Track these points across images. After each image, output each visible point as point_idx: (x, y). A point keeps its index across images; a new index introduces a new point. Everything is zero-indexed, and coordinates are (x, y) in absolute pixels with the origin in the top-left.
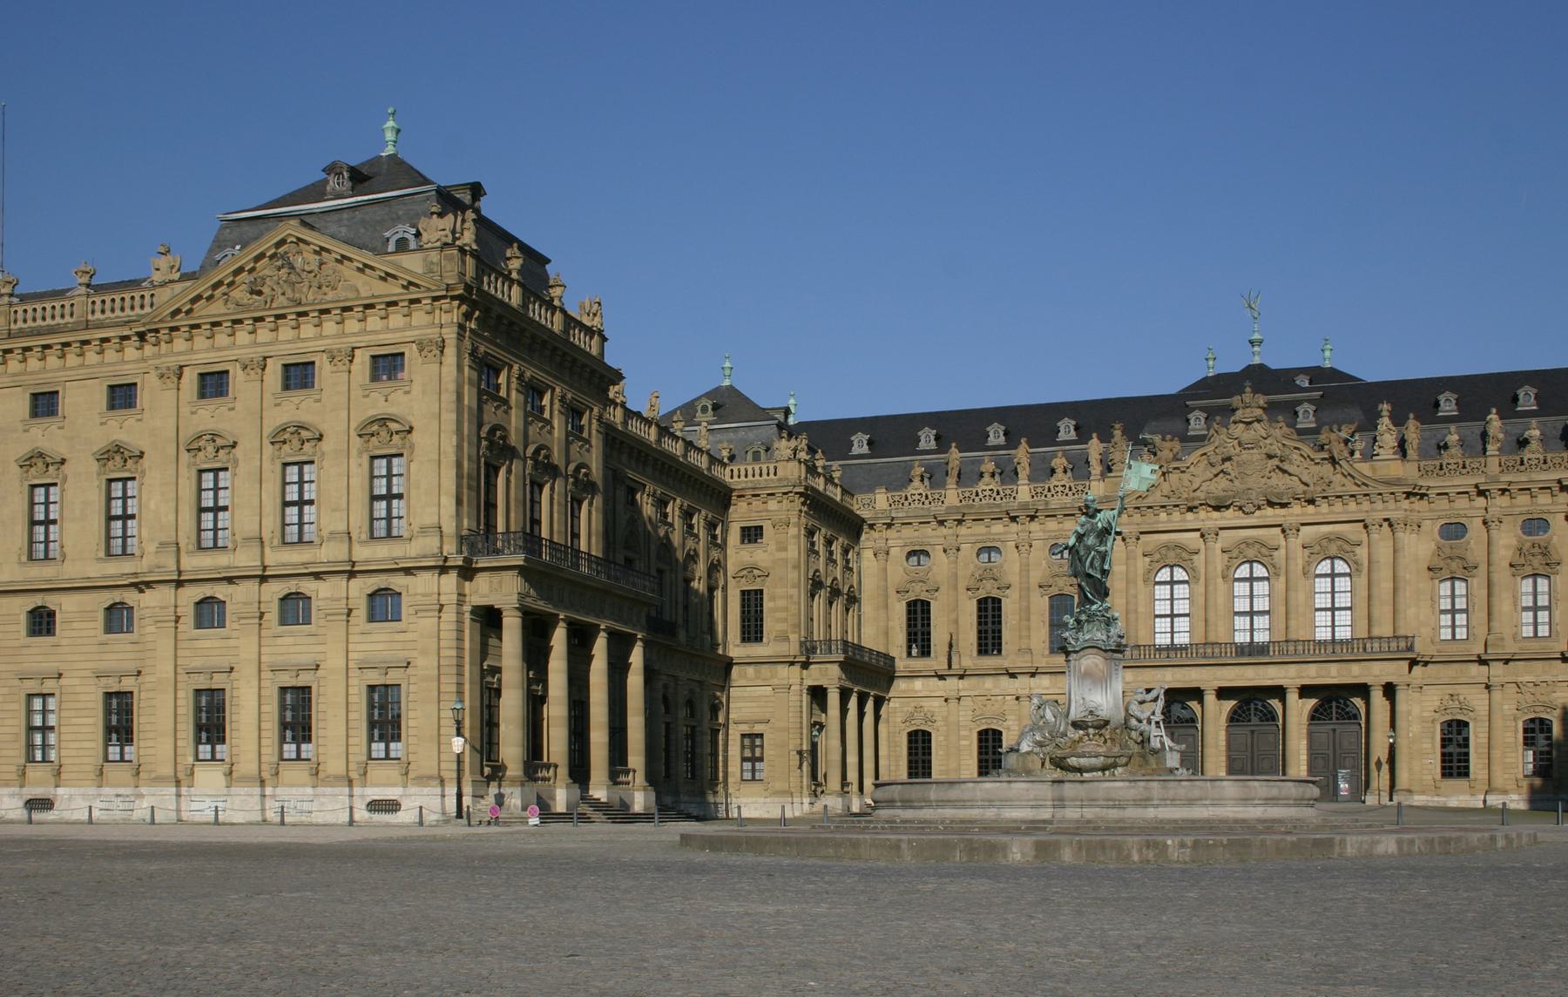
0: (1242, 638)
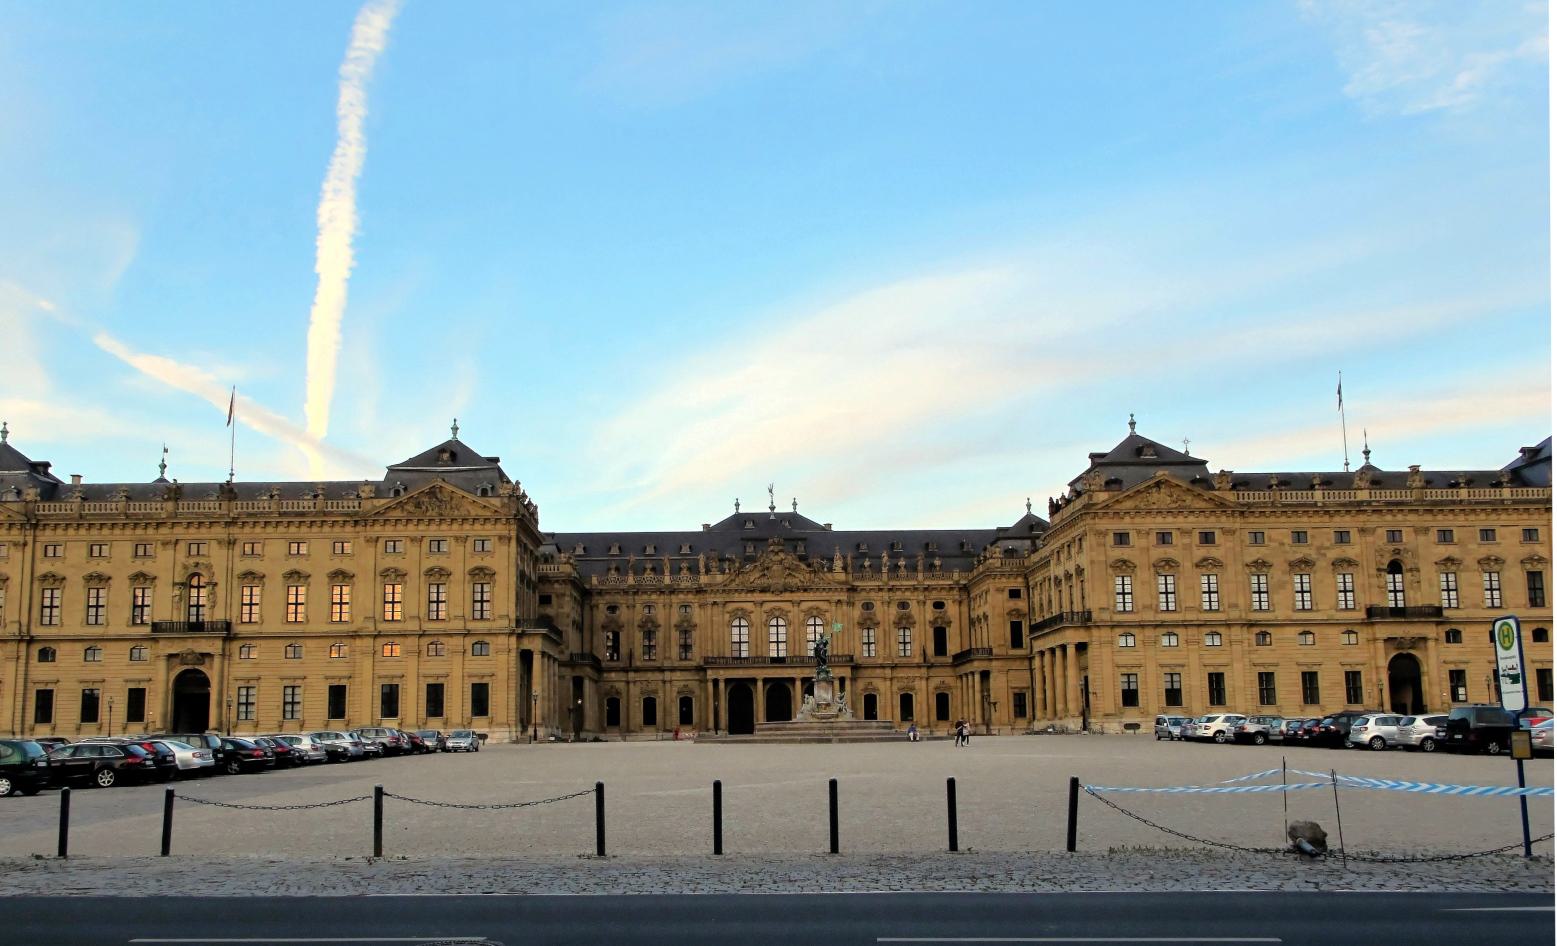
0: (773, 654)
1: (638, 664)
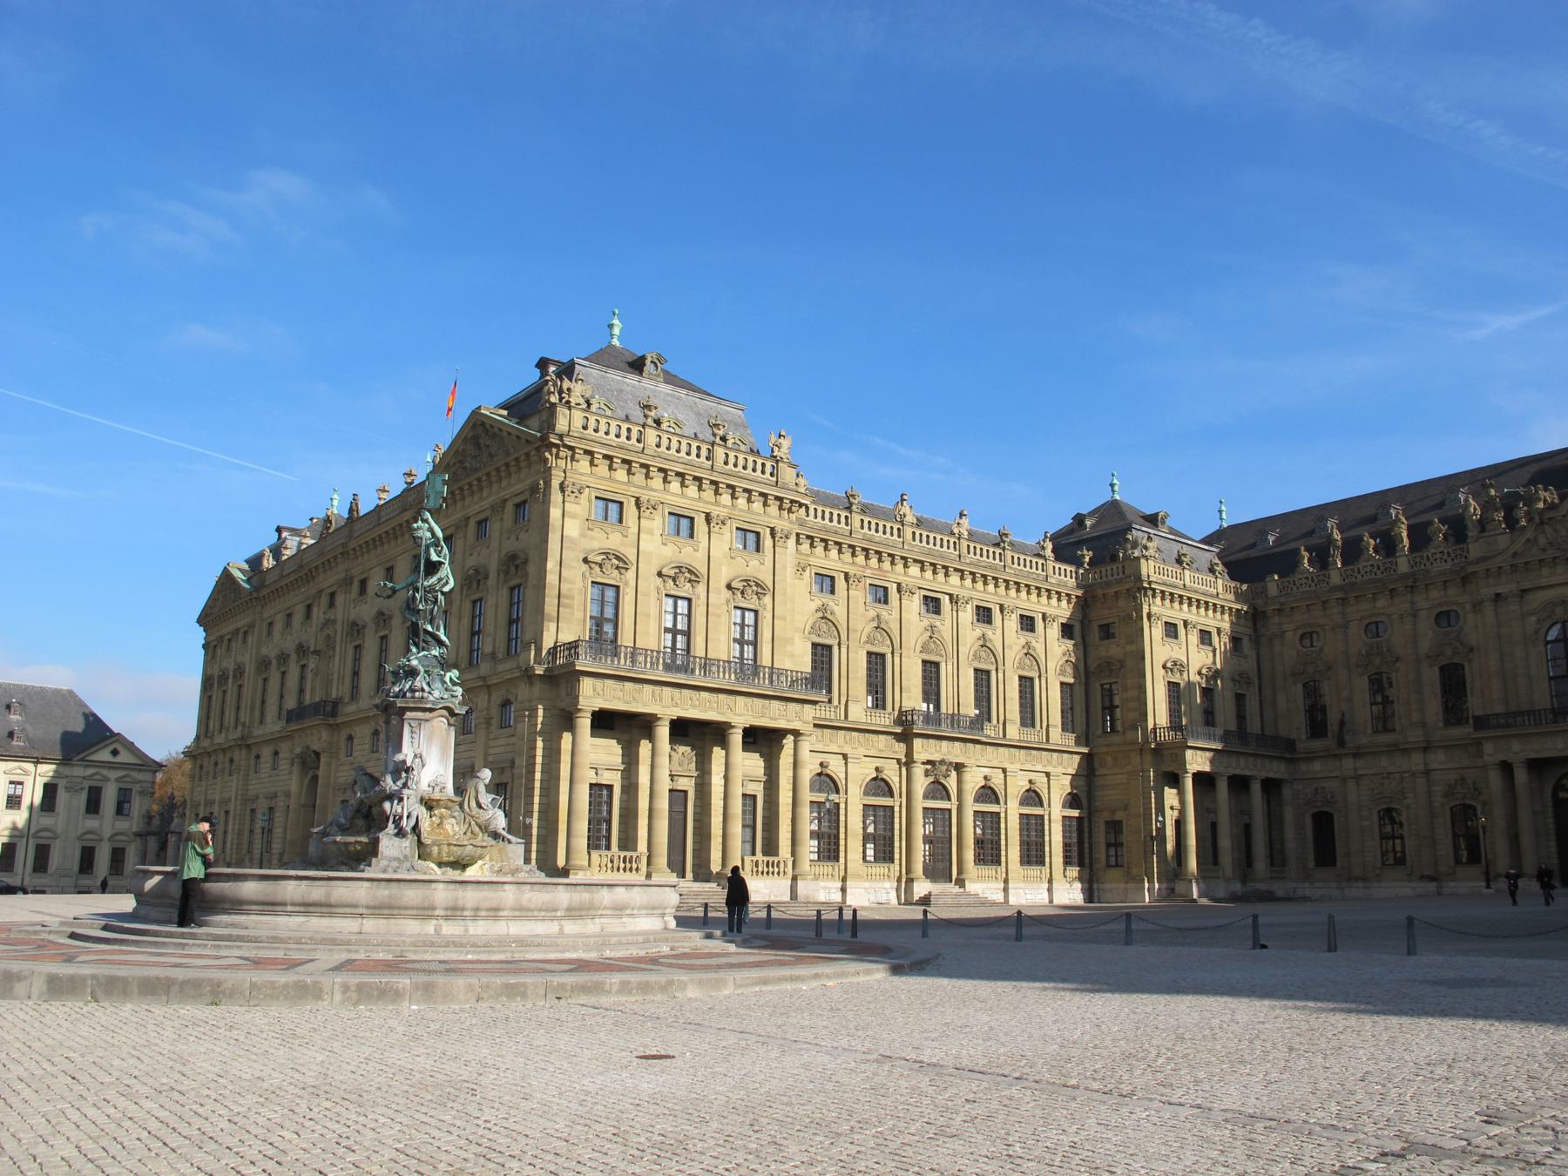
1: (1364, 741)
